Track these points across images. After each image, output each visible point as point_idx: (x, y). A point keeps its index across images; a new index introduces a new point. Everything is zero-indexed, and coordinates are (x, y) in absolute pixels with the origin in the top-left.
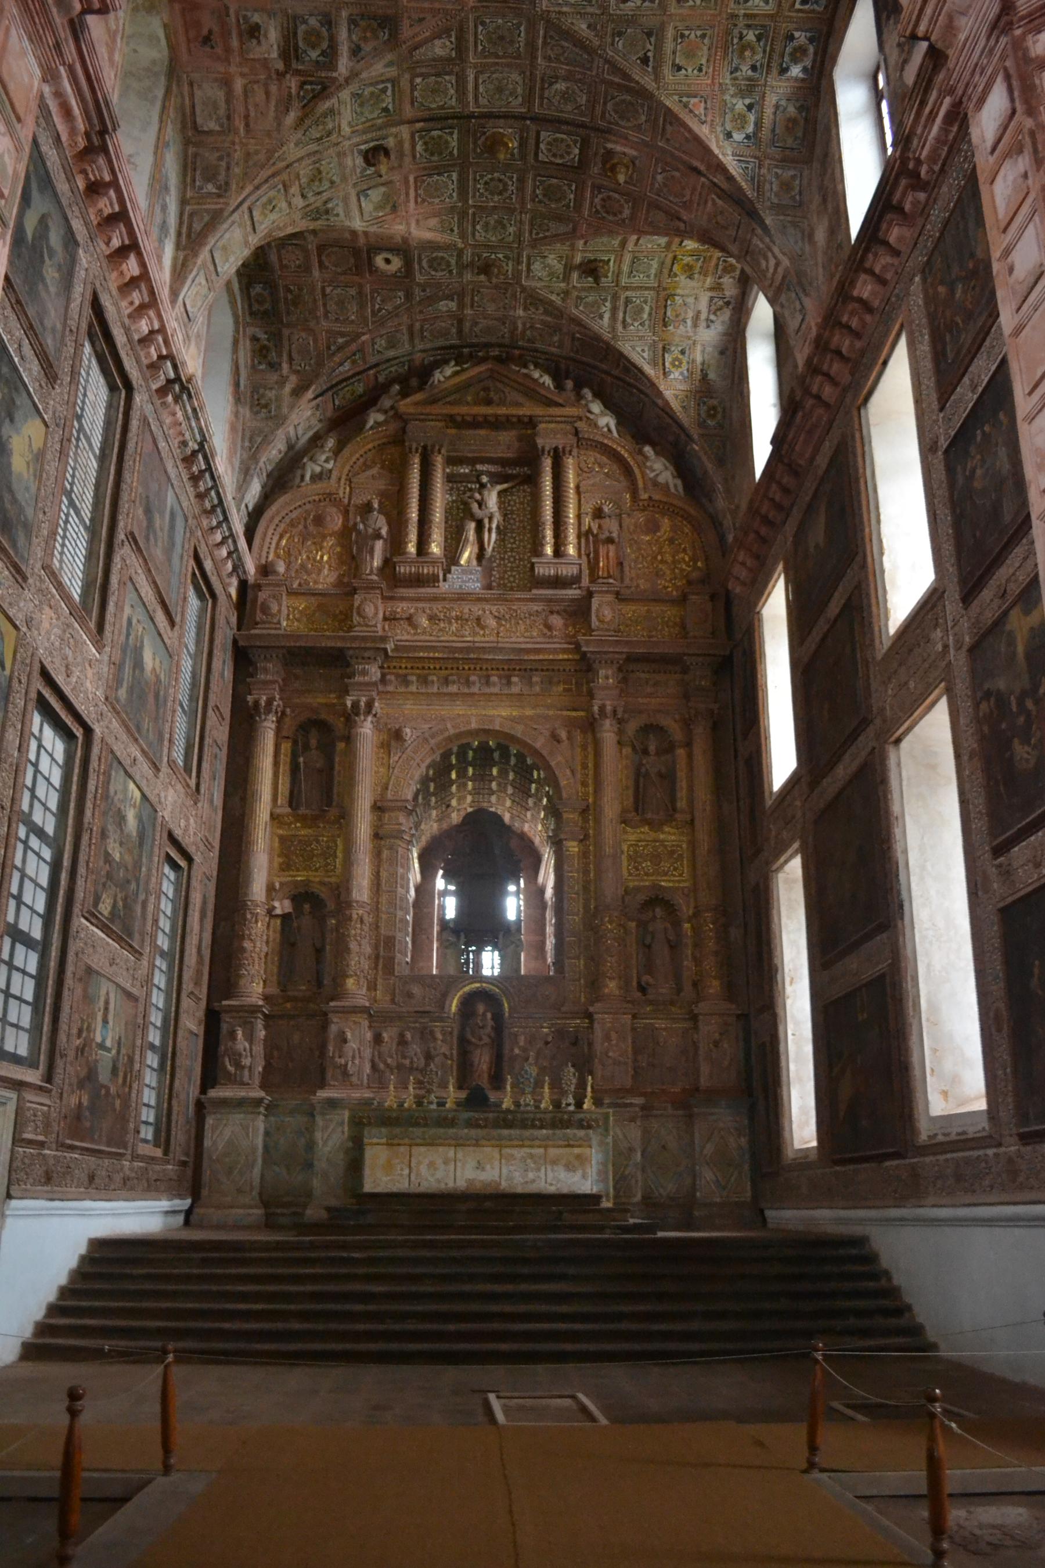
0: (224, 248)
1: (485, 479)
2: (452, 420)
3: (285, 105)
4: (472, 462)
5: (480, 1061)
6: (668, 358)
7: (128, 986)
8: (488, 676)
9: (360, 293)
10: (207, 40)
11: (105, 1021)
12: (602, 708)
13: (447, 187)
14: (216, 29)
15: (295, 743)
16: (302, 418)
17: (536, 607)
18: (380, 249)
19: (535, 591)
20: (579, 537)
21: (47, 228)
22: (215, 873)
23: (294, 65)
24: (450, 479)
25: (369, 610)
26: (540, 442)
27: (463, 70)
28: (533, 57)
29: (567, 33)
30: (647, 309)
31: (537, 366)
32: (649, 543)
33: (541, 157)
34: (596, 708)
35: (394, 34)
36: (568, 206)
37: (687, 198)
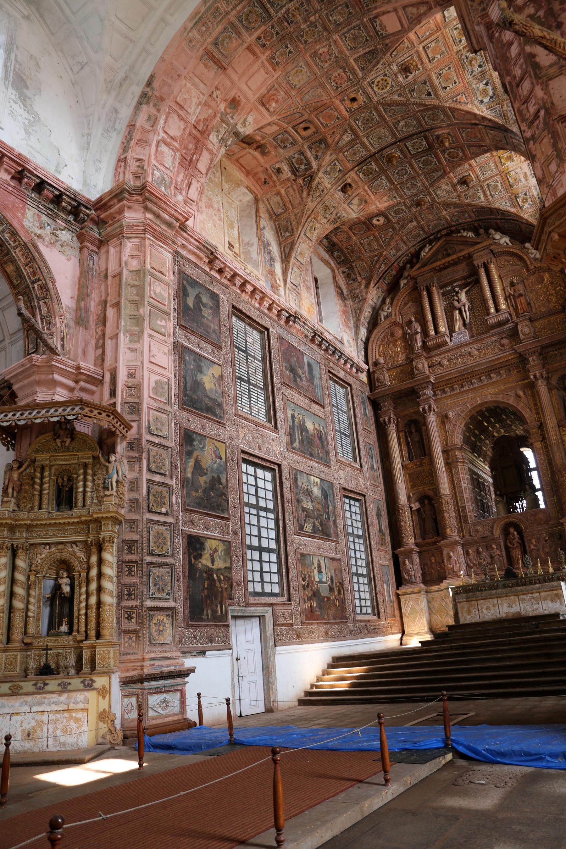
0: (301, 254)
1: (457, 289)
2: (434, 270)
4: (451, 283)
6: (519, 200)
7: (334, 555)
8: (480, 378)
9: (375, 237)
10: (265, 182)
11: (320, 571)
12: (535, 376)
13: (382, 183)
14: (266, 177)
15: (405, 432)
16: (373, 296)
18: (372, 218)
19: (491, 331)
20: (506, 299)
21: (200, 298)
22: (384, 497)
23: (297, 173)
24: (443, 294)
25: (420, 366)
26: (475, 263)
27: (361, 140)
28: (384, 119)
29: (390, 104)
30: (499, 184)
31: (464, 230)
32: (541, 287)
33: (412, 153)
34: (532, 377)
35: (326, 144)
36: (436, 164)
37: (479, 137)
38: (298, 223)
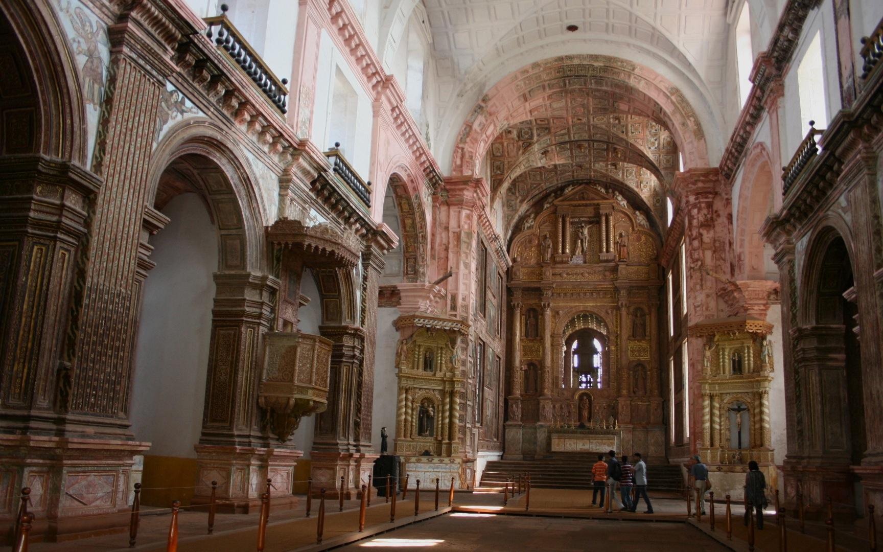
3: (519, 149)
5: (584, 412)
16: (523, 208)
17: (600, 269)
20: (614, 244)
24: (572, 223)
25: (547, 273)
38: (509, 168)
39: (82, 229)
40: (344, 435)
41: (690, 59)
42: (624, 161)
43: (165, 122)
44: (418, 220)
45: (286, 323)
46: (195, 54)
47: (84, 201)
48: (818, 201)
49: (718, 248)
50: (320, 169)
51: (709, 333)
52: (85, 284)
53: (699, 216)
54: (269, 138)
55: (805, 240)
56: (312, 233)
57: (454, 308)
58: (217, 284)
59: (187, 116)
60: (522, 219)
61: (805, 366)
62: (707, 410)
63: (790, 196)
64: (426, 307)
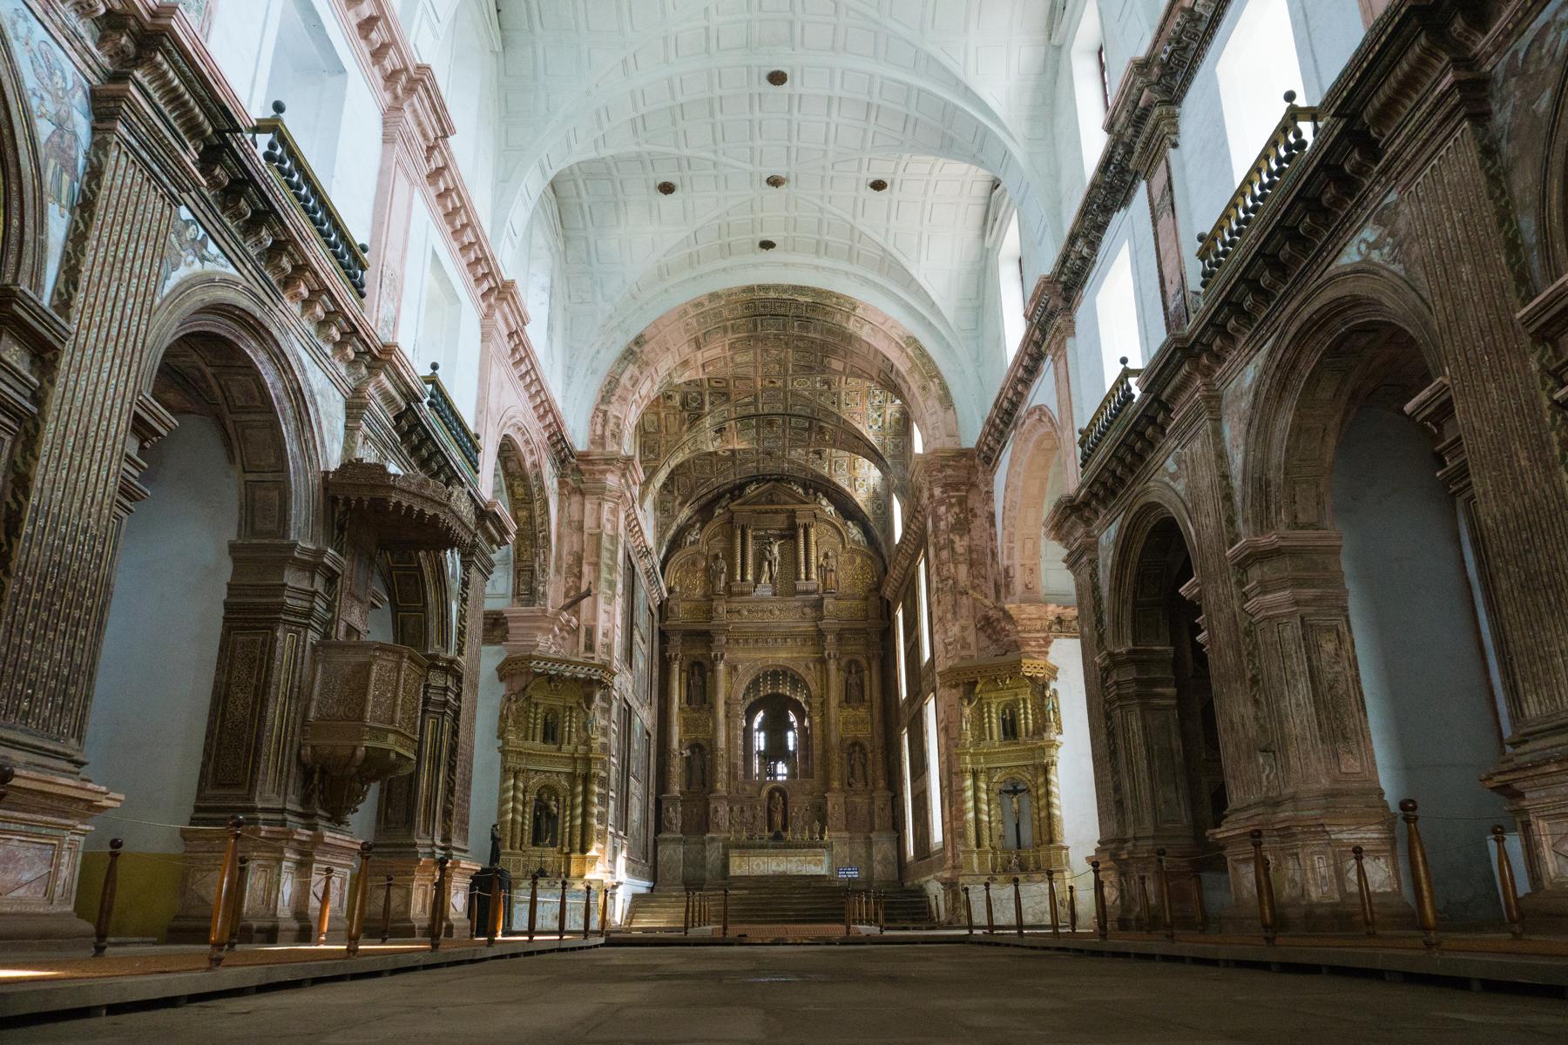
16: (685, 513)
24: (755, 538)
25: (720, 610)
39: (28, 405)
40: (426, 832)
41: (934, 297)
42: (833, 446)
43: (175, 267)
44: (538, 512)
45: (351, 630)
46: (229, 168)
47: (32, 363)
48: (1132, 471)
49: (979, 559)
50: (412, 397)
51: (966, 682)
52: (27, 499)
53: (947, 516)
54: (335, 333)
55: (1113, 529)
56: (404, 485)
57: (590, 647)
58: (235, 560)
59: (209, 267)
60: (682, 531)
61: (1121, 707)
62: (970, 793)
63: (1093, 466)
64: (546, 644)
